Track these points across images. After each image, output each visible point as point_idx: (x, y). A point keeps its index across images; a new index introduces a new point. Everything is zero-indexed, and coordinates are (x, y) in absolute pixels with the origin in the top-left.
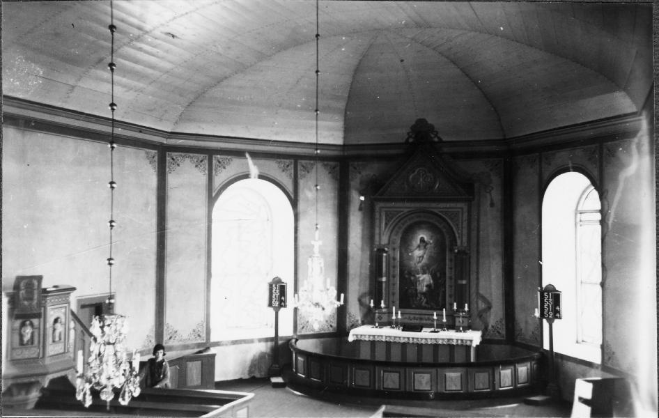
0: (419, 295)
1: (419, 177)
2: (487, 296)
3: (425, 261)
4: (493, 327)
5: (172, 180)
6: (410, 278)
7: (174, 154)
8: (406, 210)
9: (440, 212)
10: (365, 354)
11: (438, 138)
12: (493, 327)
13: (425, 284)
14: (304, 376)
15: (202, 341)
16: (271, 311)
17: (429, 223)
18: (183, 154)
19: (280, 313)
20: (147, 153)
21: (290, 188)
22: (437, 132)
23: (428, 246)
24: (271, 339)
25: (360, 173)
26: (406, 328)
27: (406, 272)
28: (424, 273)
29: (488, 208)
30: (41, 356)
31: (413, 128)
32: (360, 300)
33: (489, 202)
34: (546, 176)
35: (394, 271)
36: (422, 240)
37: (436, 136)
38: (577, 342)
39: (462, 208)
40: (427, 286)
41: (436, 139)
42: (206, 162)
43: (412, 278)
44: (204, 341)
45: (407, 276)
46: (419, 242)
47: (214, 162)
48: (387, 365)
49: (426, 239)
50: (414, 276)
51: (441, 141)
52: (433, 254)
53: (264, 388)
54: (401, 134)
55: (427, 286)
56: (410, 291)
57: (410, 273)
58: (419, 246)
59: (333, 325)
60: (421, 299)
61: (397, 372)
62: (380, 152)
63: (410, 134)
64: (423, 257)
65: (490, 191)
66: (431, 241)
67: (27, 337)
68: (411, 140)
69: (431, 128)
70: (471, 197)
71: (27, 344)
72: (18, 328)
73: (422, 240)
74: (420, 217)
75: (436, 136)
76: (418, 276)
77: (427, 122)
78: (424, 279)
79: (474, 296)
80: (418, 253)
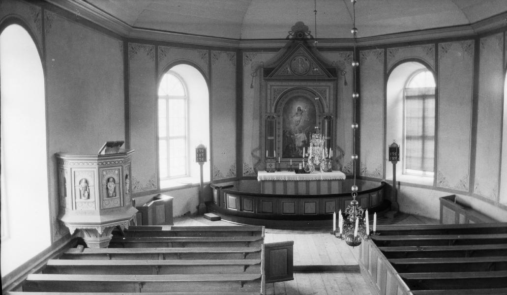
0: (297, 148)
1: (301, 63)
2: (343, 148)
3: (301, 124)
4: (345, 167)
5: (132, 65)
6: (290, 136)
7: (134, 45)
8: (291, 87)
9: (314, 89)
10: (268, 191)
11: (311, 36)
12: (345, 167)
13: (301, 140)
14: (236, 210)
15: (155, 189)
16: (198, 165)
17: (303, 96)
18: (140, 44)
19: (397, 165)
20: (119, 43)
21: (206, 70)
22: (310, 32)
23: (303, 114)
24: (198, 186)
25: (251, 60)
26: (297, 171)
27: (288, 133)
28: (301, 132)
29: (344, 86)
30: (122, 205)
31: (294, 28)
32: (252, 154)
33: (344, 82)
34: (389, 66)
35: (279, 131)
36: (299, 109)
37: (309, 34)
38: (403, 174)
39: (329, 86)
40: (302, 142)
41: (309, 37)
42: (154, 51)
43: (292, 136)
44: (157, 189)
45: (288, 135)
46: (297, 110)
47: (159, 51)
48: (308, 197)
49: (302, 109)
50: (293, 135)
51: (312, 38)
52: (306, 119)
53: (186, 221)
54: (284, 33)
55: (302, 142)
56: (290, 146)
57: (290, 133)
58: (297, 113)
59: (234, 172)
60: (298, 151)
61: (313, 202)
62: (266, 45)
63: (291, 33)
64: (300, 121)
65: (344, 74)
66: (306, 110)
67: (111, 192)
68: (291, 37)
69: (306, 28)
70: (336, 78)
71: (113, 196)
72: (106, 184)
73: (299, 109)
74: (298, 92)
75: (309, 34)
76: (296, 135)
77: (303, 24)
78: (300, 137)
79: (334, 146)
80: (297, 118)
